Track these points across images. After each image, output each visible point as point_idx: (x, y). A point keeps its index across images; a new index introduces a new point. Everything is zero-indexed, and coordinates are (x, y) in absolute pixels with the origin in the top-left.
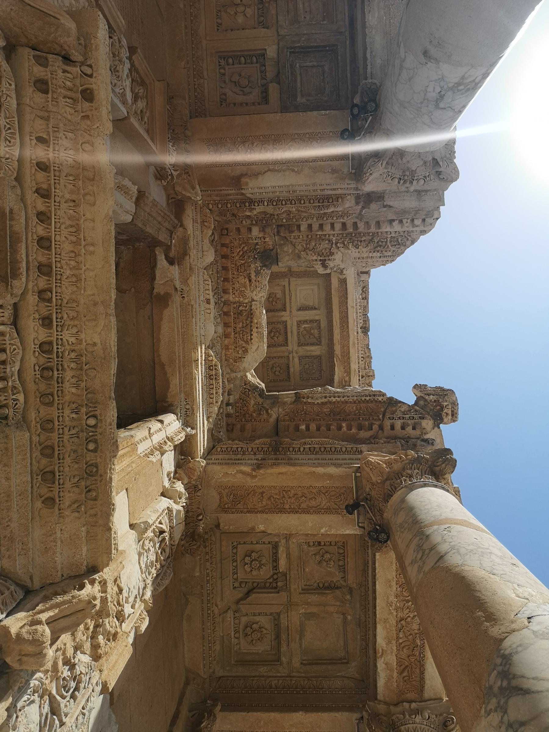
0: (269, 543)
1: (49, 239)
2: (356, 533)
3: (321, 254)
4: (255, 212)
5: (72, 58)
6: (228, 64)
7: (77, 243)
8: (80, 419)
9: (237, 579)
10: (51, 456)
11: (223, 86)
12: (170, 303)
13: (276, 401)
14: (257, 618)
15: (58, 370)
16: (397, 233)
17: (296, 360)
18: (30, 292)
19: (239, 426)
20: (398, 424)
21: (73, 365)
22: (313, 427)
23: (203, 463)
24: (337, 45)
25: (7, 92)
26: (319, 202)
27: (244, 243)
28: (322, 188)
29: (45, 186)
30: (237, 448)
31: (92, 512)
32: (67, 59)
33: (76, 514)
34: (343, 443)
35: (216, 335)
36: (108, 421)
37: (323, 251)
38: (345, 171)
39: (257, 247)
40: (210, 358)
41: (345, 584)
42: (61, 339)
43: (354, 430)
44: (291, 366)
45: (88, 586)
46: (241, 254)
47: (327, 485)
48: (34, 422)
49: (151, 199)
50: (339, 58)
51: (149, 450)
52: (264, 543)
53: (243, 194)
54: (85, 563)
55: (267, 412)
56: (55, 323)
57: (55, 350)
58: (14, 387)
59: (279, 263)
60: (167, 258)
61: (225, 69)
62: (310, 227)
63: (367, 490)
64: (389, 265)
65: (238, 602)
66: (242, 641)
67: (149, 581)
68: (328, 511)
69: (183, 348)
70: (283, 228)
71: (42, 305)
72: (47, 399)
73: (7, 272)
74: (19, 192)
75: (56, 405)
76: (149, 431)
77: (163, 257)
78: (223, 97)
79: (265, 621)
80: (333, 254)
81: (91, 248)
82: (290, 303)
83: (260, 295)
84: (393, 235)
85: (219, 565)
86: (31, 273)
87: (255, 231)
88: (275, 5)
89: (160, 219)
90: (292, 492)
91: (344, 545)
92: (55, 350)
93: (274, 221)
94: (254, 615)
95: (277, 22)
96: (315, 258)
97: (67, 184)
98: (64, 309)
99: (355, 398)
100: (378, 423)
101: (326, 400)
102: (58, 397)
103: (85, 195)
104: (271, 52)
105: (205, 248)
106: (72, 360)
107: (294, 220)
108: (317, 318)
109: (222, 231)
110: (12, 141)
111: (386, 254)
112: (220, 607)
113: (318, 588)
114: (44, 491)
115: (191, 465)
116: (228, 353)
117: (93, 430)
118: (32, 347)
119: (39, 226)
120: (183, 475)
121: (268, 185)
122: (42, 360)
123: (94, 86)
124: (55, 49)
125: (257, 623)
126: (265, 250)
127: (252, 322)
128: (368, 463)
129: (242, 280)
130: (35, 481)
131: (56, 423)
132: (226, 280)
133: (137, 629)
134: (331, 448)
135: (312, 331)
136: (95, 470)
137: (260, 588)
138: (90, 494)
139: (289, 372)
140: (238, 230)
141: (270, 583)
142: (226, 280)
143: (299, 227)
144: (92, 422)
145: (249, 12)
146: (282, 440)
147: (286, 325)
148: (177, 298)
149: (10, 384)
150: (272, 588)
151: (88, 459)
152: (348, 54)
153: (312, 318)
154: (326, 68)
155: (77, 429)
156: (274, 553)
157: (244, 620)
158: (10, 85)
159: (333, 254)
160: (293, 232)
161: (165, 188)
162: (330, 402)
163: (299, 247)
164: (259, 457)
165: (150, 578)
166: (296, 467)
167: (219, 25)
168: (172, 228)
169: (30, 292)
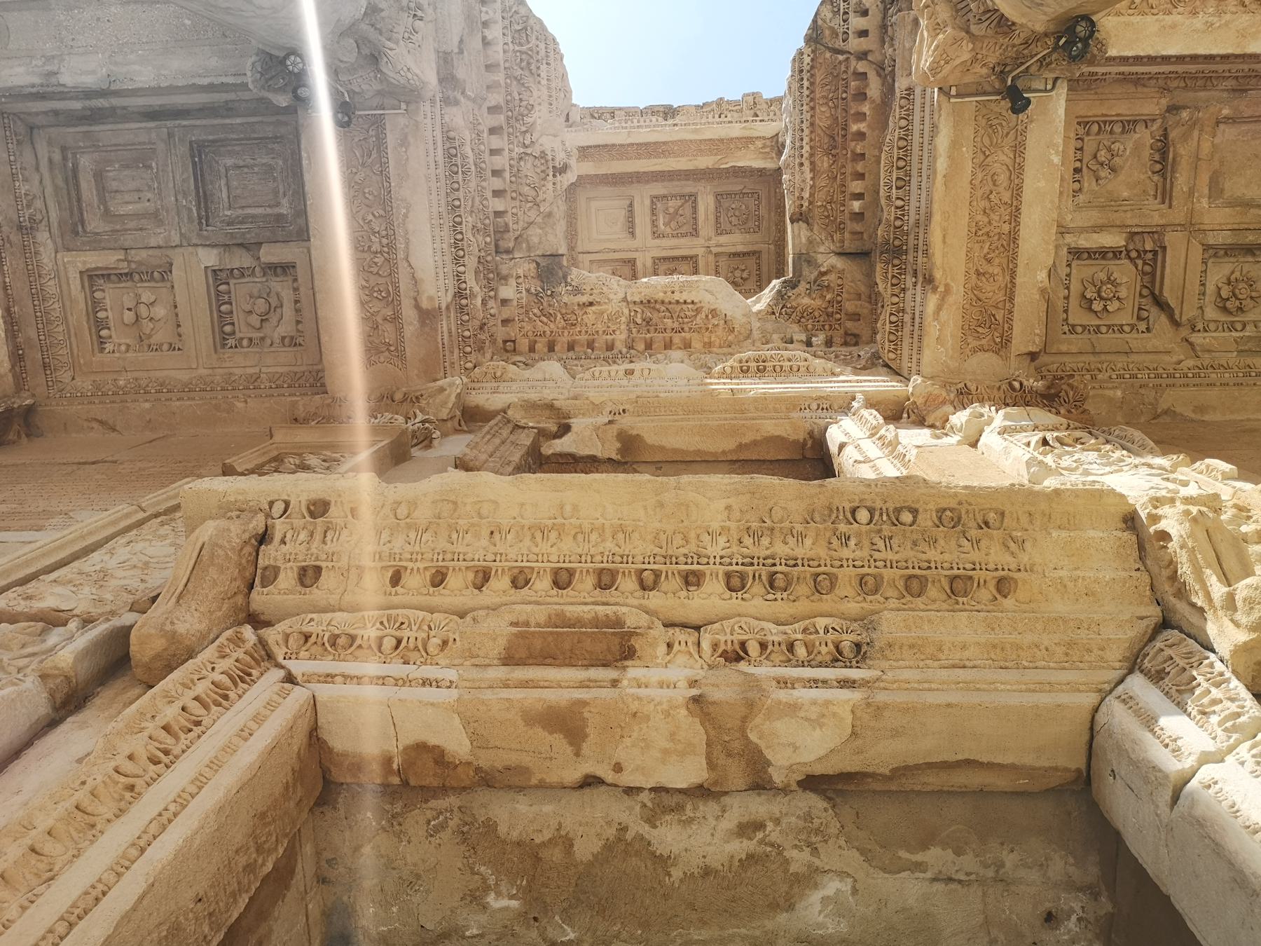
0: (1069, 265)
1: (556, 572)
2: (1064, 96)
3: (543, 175)
4: (477, 289)
5: (261, 531)
6: (234, 333)
7: (560, 530)
8: (859, 535)
9: (1133, 327)
10: (923, 581)
11: (269, 342)
12: (634, 432)
13: (804, 259)
14: (1210, 288)
15: (774, 565)
17: (723, 239)
18: (643, 602)
19: (849, 324)
20: (857, 22)
21: (765, 541)
22: (856, 186)
23: (916, 380)
24: (191, 142)
25: (325, 624)
26: (457, 173)
28: (432, 165)
29: (471, 576)
30: (891, 323)
31: (1024, 520)
32: (263, 538)
33: (1028, 545)
34: (891, 124)
35: (687, 361)
36: (864, 489)
37: (539, 171)
38: (402, 121)
40: (728, 370)
41: (1159, 121)
42: (722, 557)
43: (866, 108)
44: (733, 250)
45: (1163, 525)
46: (545, 319)
47: (971, 153)
48: (864, 605)
49: (468, 451)
50: (211, 138)
51: (896, 462)
52: (1068, 275)
53: (448, 308)
54: (1119, 534)
55: (825, 274)
56: (695, 567)
57: (739, 568)
58: (805, 631)
59: (560, 252)
61: (242, 339)
62: (497, 193)
63: (984, 71)
64: (563, 49)
65: (1176, 324)
66: (1250, 317)
67: (1138, 460)
68: (1019, 150)
69: (712, 412)
70: (501, 243)
71: (664, 585)
72: (822, 584)
73: (613, 634)
74: (482, 613)
75: (834, 570)
76: (860, 462)
77: (557, 441)
78: (287, 341)
79: (1218, 274)
80: (543, 152)
81: (568, 508)
82: (620, 250)
83: (615, 286)
85: (1103, 357)
86: (612, 600)
87: (507, 292)
88: (133, 252)
89: (497, 441)
90: (979, 217)
91: (1084, 123)
92: (739, 568)
93: (489, 258)
94: (1204, 294)
95: (160, 247)
96: (550, 186)
97: (465, 542)
98: (670, 552)
99: (805, 107)
100: (853, 62)
101: (807, 164)
102: (820, 566)
103: (481, 517)
104: (209, 258)
105: (540, 376)
106: (757, 542)
107: (487, 221)
108: (647, 202)
109: (508, 348)
110: (400, 620)
111: (542, 53)
112: (1182, 357)
113: (1162, 173)
114: (985, 594)
115: (920, 401)
116: (717, 344)
117: (877, 513)
118: (734, 603)
119: (534, 587)
120: (939, 413)
121: (431, 261)
122: (758, 589)
123: (304, 498)
124: (250, 554)
125: (1219, 289)
126: (539, 277)
128: (935, 69)
129: (590, 316)
130: (967, 607)
131: (866, 570)
132: (590, 345)
133: (1226, 477)
134: (900, 148)
135: (671, 210)
136: (948, 513)
137: (1153, 282)
138: (991, 522)
139: (744, 254)
140: (505, 322)
141: (1145, 263)
143: (498, 214)
144: (863, 515)
145: (147, 297)
146: (880, 240)
147: (659, 259)
148: (626, 422)
149: (799, 636)
150: (1155, 260)
151: (930, 523)
152: (204, 122)
153: (648, 211)
154: (230, 162)
155: (877, 540)
156: (1090, 257)
157: (1211, 313)
158: (312, 620)
159: (543, 152)
160: (506, 225)
161: (444, 435)
162: (812, 155)
163: (533, 214)
164: (910, 280)
165: (1129, 460)
166: (934, 211)
167: (172, 347)
168: (510, 426)
169: (643, 602)
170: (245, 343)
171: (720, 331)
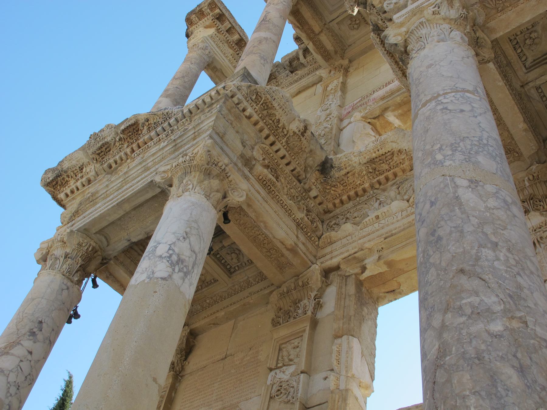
3: (299, 140)
6: (231, 267)
11: (244, 264)
16: (252, 105)
27: (325, 191)
39: (322, 181)
46: (333, 188)
60: (362, 273)
62: (288, 164)
77: (364, 274)
83: (354, 158)
84: (255, 105)
87: (313, 193)
96: (305, 142)
111: (270, 99)
127: (376, 158)
129: (351, 179)
132: (357, 194)
140: (320, 204)
142: (357, 194)
143: (292, 171)
170: (237, 268)
171: (407, 163)
